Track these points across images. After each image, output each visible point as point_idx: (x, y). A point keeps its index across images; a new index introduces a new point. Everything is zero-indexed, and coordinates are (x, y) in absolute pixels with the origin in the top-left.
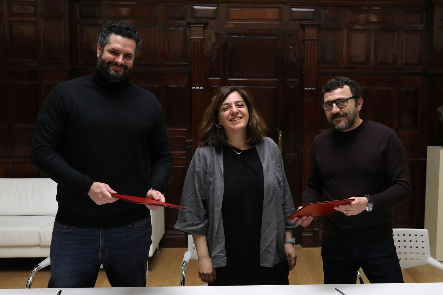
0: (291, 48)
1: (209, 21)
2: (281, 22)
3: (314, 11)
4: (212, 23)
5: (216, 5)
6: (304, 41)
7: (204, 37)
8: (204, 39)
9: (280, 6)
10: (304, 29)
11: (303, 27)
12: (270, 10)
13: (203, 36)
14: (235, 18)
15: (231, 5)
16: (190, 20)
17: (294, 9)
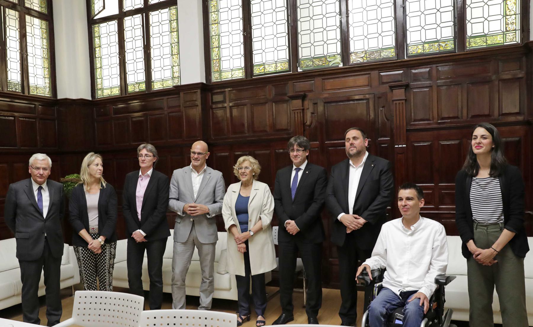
0: (382, 110)
1: (307, 93)
2: (371, 87)
3: (403, 72)
4: (310, 95)
5: (313, 79)
6: (393, 101)
7: (302, 108)
8: (303, 109)
9: (370, 72)
10: (392, 91)
11: (392, 88)
12: (361, 77)
13: (303, 107)
14: (329, 88)
15: (323, 78)
16: (290, 94)
17: (382, 74)
